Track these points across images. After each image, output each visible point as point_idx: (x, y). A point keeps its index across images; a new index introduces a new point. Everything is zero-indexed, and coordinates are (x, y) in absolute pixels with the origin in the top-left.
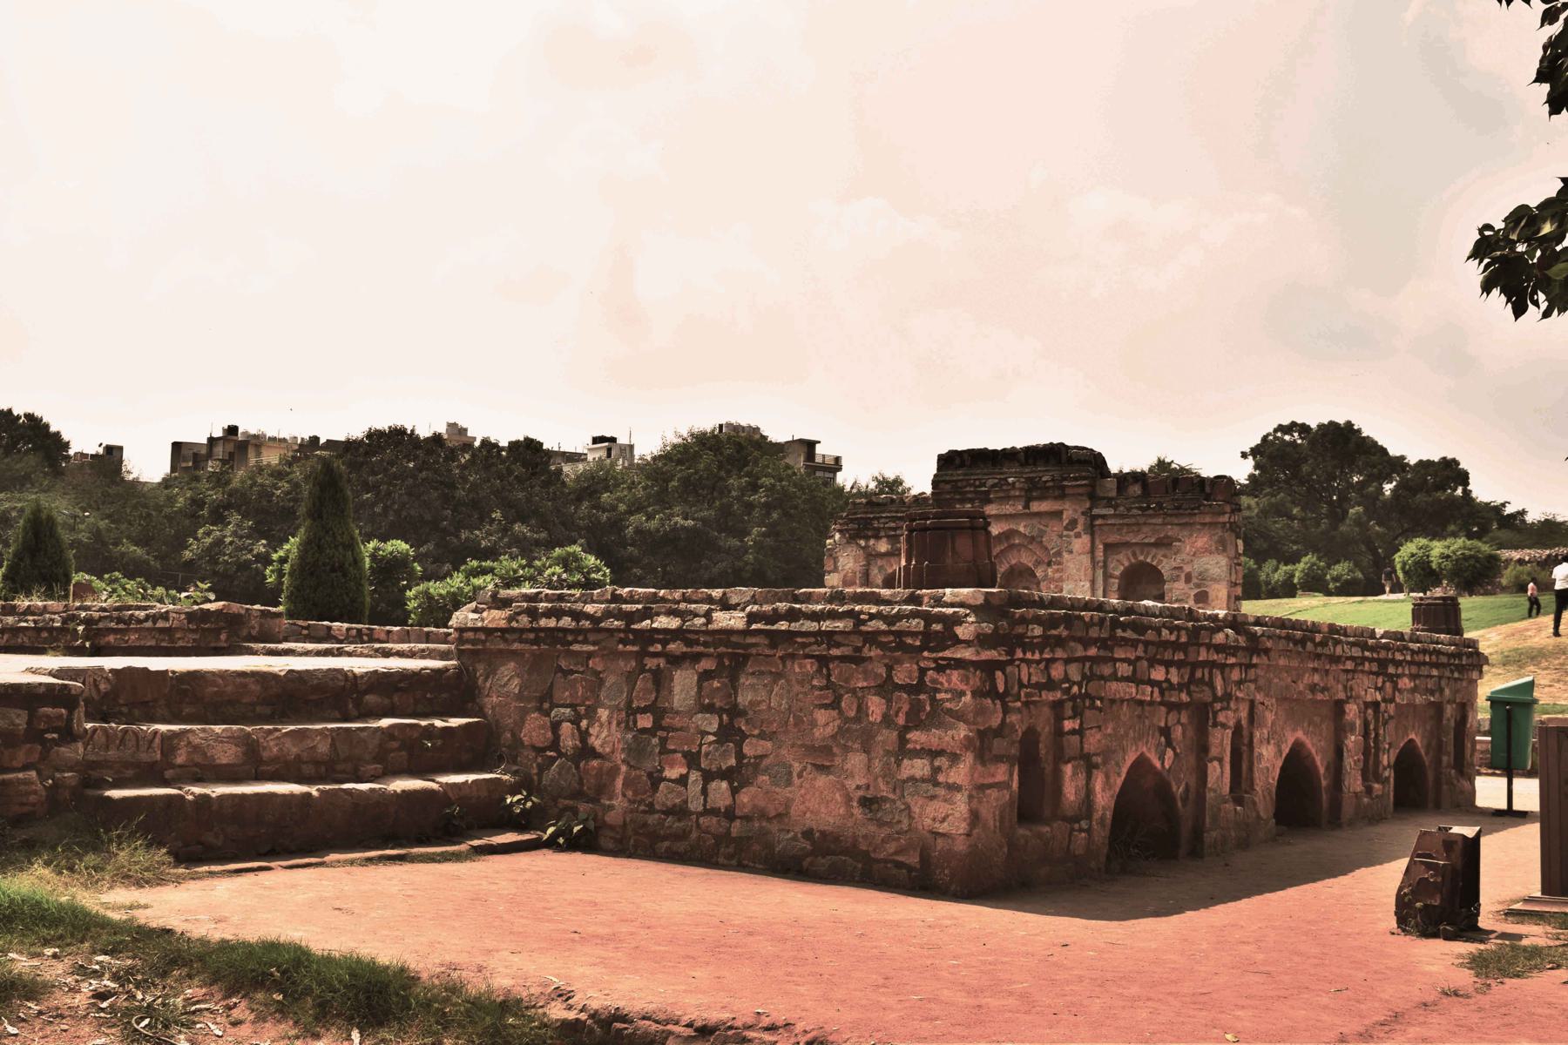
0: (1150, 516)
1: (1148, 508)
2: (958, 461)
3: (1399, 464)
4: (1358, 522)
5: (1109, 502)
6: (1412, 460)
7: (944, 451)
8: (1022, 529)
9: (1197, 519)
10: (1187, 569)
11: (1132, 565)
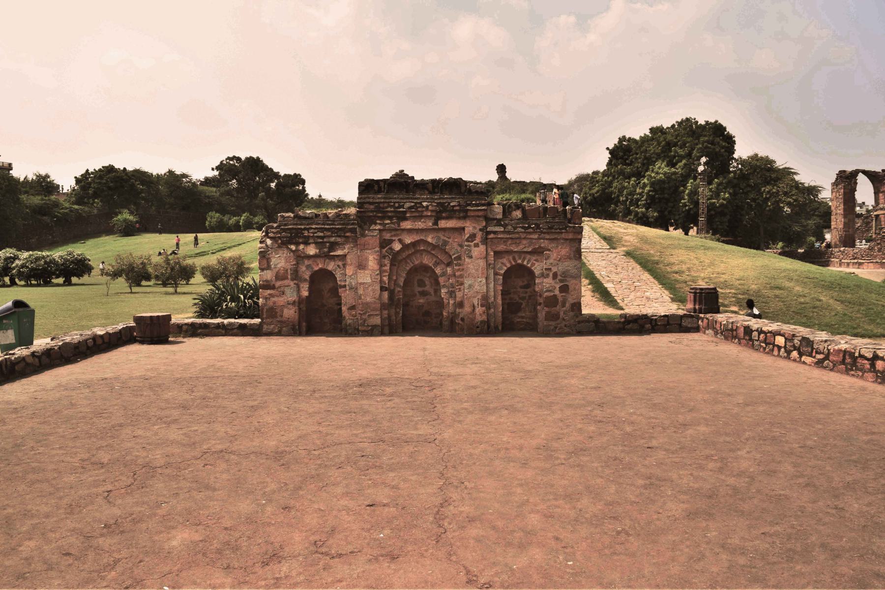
0: (530, 233)
1: (529, 227)
2: (376, 187)
3: (276, 175)
4: (263, 199)
5: (498, 222)
6: (282, 174)
7: (362, 180)
8: (429, 240)
9: (563, 236)
10: (554, 269)
11: (512, 266)
